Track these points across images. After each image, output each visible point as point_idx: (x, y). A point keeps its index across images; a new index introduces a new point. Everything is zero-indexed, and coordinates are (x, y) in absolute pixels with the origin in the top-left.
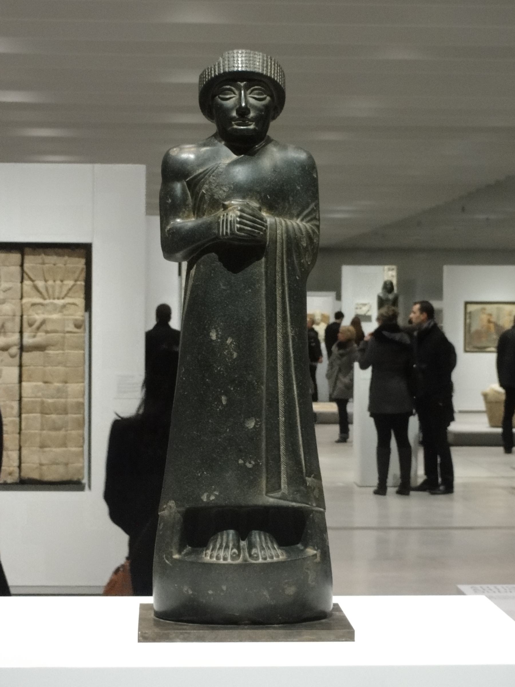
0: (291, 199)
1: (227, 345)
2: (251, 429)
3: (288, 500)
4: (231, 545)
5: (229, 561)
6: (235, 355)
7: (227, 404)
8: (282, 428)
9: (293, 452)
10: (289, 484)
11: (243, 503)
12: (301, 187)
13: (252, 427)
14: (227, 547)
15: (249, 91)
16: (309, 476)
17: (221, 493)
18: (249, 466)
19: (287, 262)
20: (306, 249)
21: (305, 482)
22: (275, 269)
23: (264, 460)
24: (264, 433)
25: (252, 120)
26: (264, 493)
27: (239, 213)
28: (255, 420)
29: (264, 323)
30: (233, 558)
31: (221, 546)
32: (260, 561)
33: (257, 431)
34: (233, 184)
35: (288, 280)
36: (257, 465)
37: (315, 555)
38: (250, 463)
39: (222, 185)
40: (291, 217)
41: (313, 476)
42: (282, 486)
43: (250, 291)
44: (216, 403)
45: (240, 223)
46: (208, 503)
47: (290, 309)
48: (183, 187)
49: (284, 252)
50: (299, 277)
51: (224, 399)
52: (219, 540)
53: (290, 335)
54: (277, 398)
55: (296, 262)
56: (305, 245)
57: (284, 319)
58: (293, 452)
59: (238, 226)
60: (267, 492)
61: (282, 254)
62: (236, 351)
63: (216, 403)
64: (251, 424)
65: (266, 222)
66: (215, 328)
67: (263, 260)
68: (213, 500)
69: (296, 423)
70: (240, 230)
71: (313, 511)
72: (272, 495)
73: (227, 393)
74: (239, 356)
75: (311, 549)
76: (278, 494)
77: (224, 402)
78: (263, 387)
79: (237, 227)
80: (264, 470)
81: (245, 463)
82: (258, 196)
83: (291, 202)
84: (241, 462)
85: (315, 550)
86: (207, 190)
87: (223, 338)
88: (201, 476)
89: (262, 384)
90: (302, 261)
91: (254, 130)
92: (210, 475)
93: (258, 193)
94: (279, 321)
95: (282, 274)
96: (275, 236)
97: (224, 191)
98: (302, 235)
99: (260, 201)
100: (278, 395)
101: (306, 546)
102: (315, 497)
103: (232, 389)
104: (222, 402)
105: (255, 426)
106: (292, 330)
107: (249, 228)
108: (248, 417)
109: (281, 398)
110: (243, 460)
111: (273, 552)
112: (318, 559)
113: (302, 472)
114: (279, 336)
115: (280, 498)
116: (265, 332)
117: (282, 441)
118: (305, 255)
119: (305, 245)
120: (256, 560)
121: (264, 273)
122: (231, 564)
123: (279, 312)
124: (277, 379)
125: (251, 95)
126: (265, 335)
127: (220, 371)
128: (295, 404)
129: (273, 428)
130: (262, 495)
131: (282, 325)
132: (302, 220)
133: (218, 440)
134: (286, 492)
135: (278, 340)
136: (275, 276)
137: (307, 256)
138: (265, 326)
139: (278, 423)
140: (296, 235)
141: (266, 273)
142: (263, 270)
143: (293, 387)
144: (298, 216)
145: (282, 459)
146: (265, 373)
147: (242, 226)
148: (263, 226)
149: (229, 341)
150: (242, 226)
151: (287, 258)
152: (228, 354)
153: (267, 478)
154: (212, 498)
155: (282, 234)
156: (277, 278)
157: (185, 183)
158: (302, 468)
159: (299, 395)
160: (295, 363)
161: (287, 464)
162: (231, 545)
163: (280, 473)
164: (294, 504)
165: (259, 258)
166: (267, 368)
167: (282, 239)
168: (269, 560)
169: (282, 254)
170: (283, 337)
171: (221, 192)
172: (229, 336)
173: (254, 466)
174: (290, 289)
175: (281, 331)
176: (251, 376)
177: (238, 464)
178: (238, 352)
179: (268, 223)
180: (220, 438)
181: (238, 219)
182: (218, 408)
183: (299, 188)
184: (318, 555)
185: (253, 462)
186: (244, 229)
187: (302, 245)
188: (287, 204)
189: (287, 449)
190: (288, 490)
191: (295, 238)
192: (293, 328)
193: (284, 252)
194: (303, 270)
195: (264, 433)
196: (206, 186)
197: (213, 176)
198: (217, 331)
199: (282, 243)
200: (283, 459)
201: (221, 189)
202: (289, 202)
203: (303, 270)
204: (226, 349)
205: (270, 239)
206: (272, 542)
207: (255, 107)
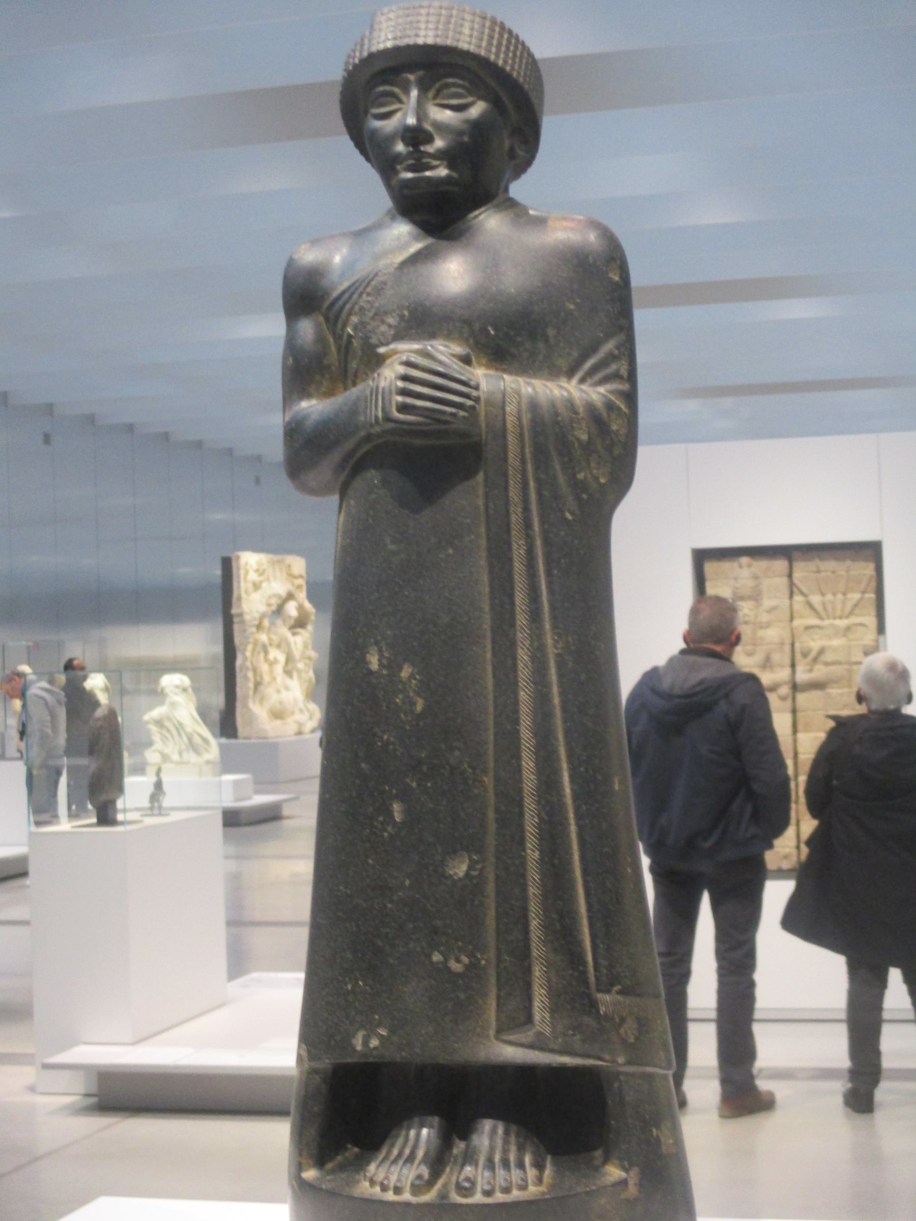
0: (551, 332)
1: (401, 681)
2: (460, 879)
3: (552, 1051)
4: (420, 1153)
5: (407, 1196)
6: (419, 706)
7: (403, 822)
8: (533, 875)
9: (562, 934)
10: (554, 1010)
11: (443, 1058)
12: (576, 304)
13: (461, 874)
14: (411, 1159)
15: (431, 94)
16: (608, 991)
17: (392, 1032)
18: (455, 967)
19: (538, 480)
20: (588, 448)
21: (593, 1005)
22: (507, 496)
23: (492, 954)
24: (491, 888)
25: (441, 155)
26: (492, 1033)
27: (402, 370)
28: (470, 857)
29: (487, 625)
30: (416, 1189)
31: (400, 1155)
32: (478, 1198)
33: (473, 886)
34: (408, 308)
35: (542, 522)
36: (473, 966)
37: (624, 1183)
38: (458, 961)
39: (386, 313)
40: (554, 373)
41: (617, 988)
42: (537, 1017)
43: (451, 551)
44: (381, 819)
45: (404, 392)
46: (364, 1055)
47: (551, 591)
48: (318, 326)
49: (528, 455)
50: (572, 513)
51: (397, 809)
52: (400, 1141)
53: (551, 652)
54: (520, 805)
55: (561, 479)
56: (584, 437)
57: (535, 616)
58: (562, 934)
59: (400, 399)
60: (499, 1031)
61: (523, 462)
62: (421, 697)
63: (381, 819)
64: (459, 868)
65: (477, 388)
66: (376, 643)
67: (480, 477)
68: (375, 1048)
69: (570, 862)
70: (403, 408)
71: (619, 1073)
72: (512, 1038)
73: (404, 795)
74: (427, 709)
75: (616, 1167)
76: (527, 1036)
77: (398, 817)
78: (488, 781)
79: (397, 403)
80: (493, 979)
81: (446, 960)
82: (466, 329)
83: (552, 341)
84: (437, 957)
85: (624, 1168)
86: (355, 328)
87: (392, 666)
88: (353, 991)
89: (485, 772)
90: (580, 476)
91: (447, 180)
92: (371, 988)
93: (467, 322)
94: (522, 619)
95: (526, 509)
96: (500, 418)
97: (390, 326)
98: (576, 413)
99: (471, 341)
100: (522, 799)
101: (606, 1160)
102: (624, 1042)
103: (414, 785)
104: (392, 817)
105: (467, 874)
106: (556, 642)
107: (428, 404)
108: (452, 852)
109: (530, 805)
110: (441, 953)
111: (516, 1174)
112: (633, 1190)
113: (586, 982)
114: (523, 655)
115: (531, 1046)
116: (489, 646)
117: (534, 908)
118: (588, 462)
119: (584, 437)
120: (465, 1196)
121: (482, 508)
122: (407, 1204)
123: (520, 598)
124: (518, 758)
125: (438, 101)
126: (489, 655)
127: (388, 743)
128: (567, 819)
129: (512, 877)
130: (488, 1037)
131: (531, 629)
132: (582, 380)
133: (385, 906)
134: (547, 1031)
135: (520, 665)
136: (508, 514)
137: (593, 465)
138: (489, 634)
139: (523, 864)
140: (557, 414)
141: (487, 507)
142: (481, 502)
143: (561, 777)
144: (570, 374)
145: (535, 952)
146: (491, 747)
147: (409, 400)
148: (467, 396)
149: (406, 672)
150: (409, 400)
151: (537, 468)
152: (404, 703)
153: (499, 997)
154: (374, 1043)
155: (519, 412)
156: (513, 518)
157: (321, 319)
158: (584, 973)
159: (576, 797)
160: (565, 721)
161: (549, 965)
162: (420, 1153)
163: (528, 985)
164: (566, 1060)
165: (469, 474)
166: (495, 734)
167: (521, 426)
168: (499, 1197)
169: (523, 462)
170: (533, 658)
171: (383, 328)
172: (405, 660)
173: (468, 967)
174: (547, 542)
175: (527, 643)
176: (457, 753)
177: (432, 963)
178: (425, 699)
179: (484, 386)
180: (392, 901)
181: (400, 384)
182: (386, 830)
183: (572, 307)
184: (631, 1183)
185: (465, 960)
186: (414, 407)
187: (578, 440)
188: (541, 345)
189: (547, 927)
190: (553, 1027)
191: (557, 423)
192: (560, 635)
193: (528, 455)
194: (585, 496)
195: (491, 888)
196: (354, 319)
197: (369, 294)
198: (380, 651)
199: (521, 435)
200: (537, 949)
201: (383, 322)
202: (547, 341)
203: (585, 496)
204: (401, 691)
205: (487, 426)
206: (521, 1149)
207: (441, 127)
